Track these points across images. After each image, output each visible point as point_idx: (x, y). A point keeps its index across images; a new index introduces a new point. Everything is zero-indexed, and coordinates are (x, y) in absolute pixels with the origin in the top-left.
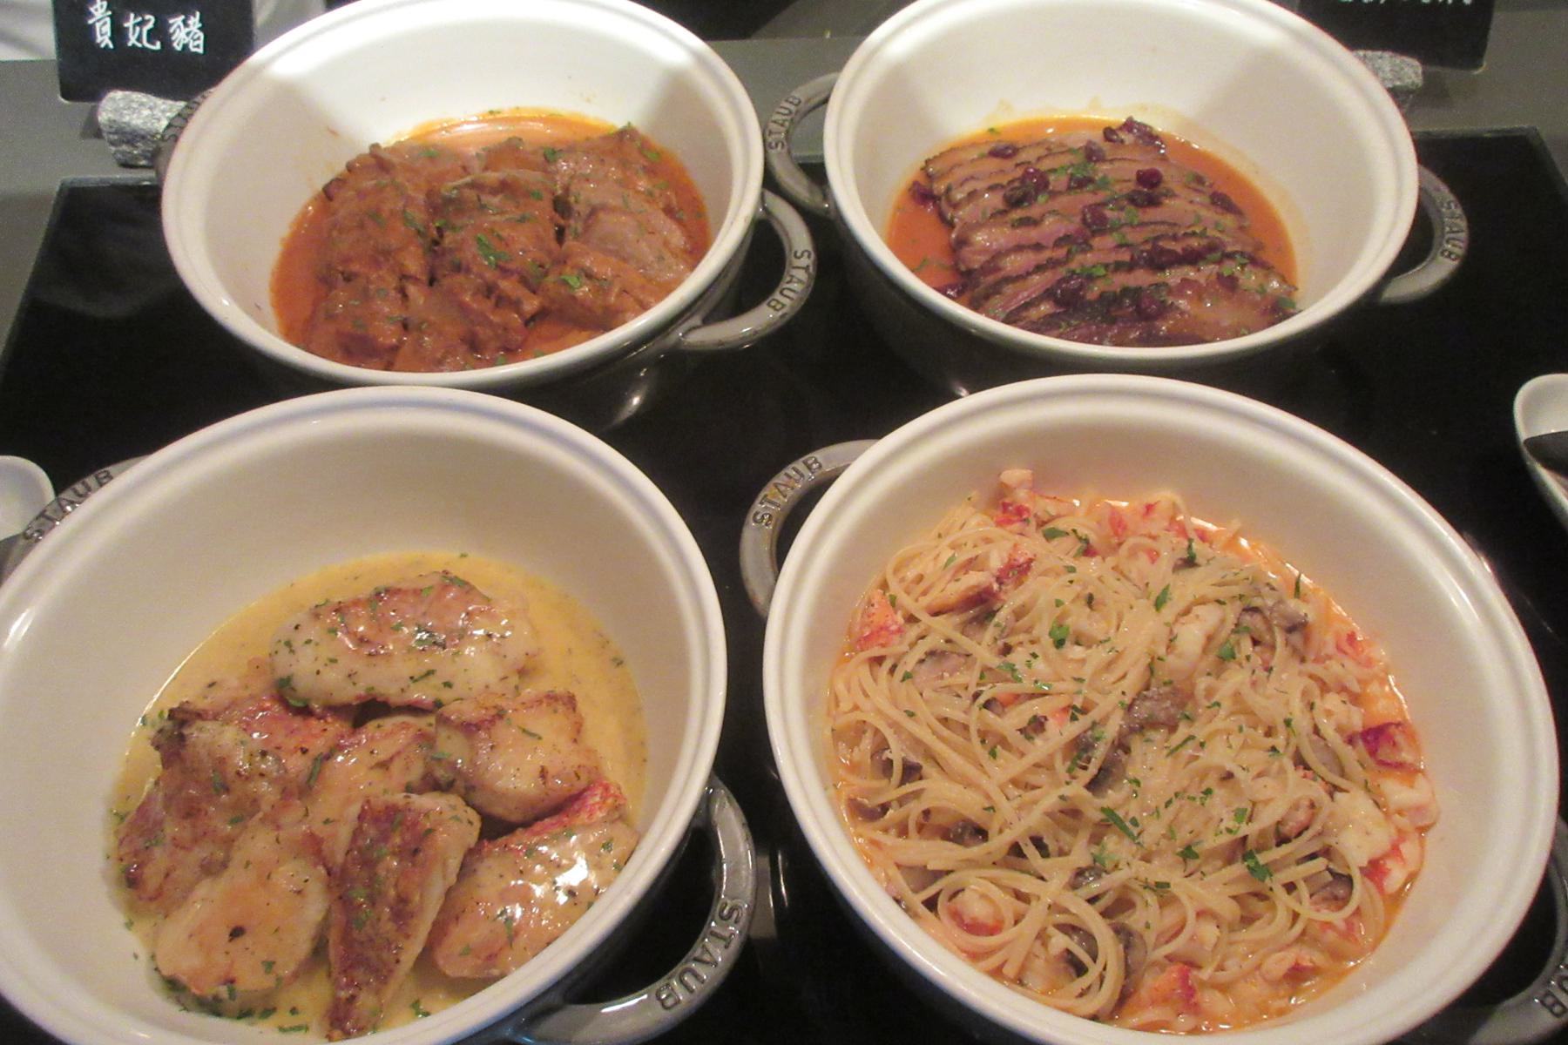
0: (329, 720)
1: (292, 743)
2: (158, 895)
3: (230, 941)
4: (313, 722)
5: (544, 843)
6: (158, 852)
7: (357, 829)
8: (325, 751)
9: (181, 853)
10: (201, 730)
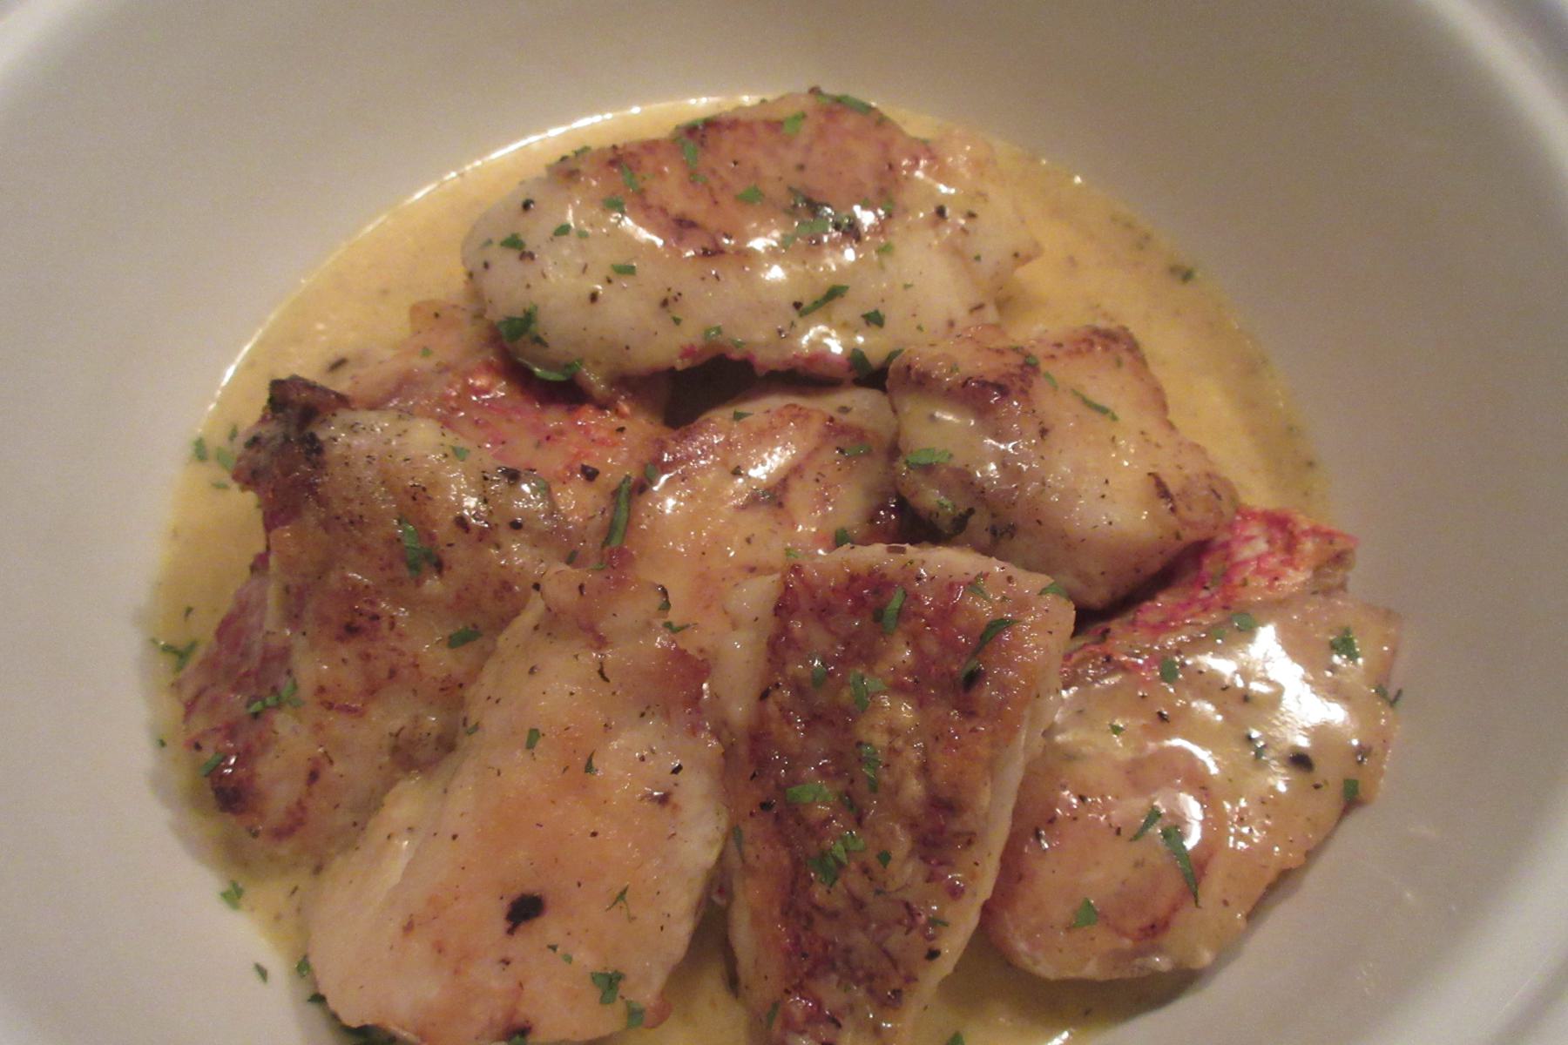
0: (626, 409)
1: (553, 460)
2: (293, 825)
3: (511, 932)
4: (588, 417)
5: (1197, 646)
6: (283, 723)
7: (778, 637)
8: (633, 473)
9: (339, 726)
10: (352, 428)
